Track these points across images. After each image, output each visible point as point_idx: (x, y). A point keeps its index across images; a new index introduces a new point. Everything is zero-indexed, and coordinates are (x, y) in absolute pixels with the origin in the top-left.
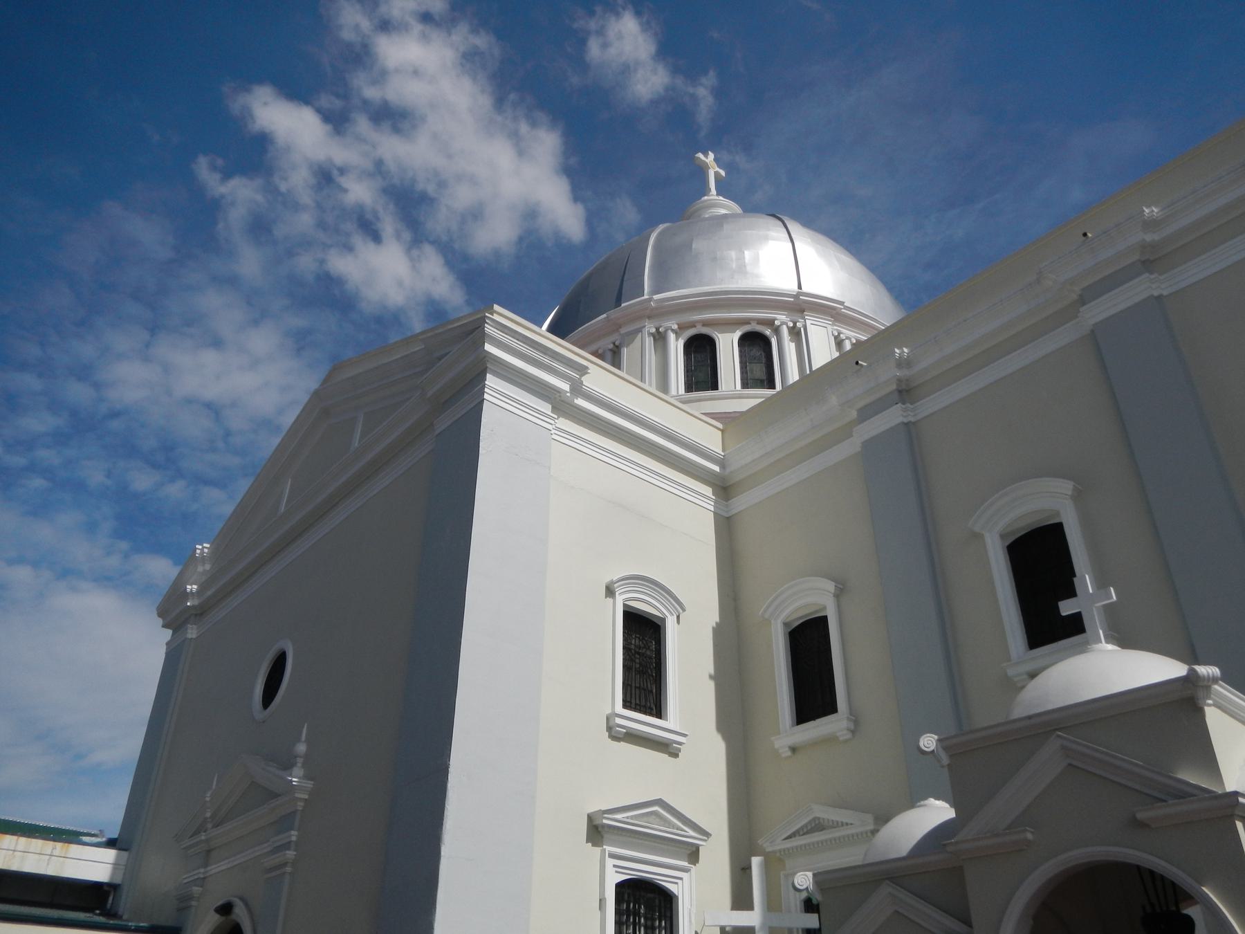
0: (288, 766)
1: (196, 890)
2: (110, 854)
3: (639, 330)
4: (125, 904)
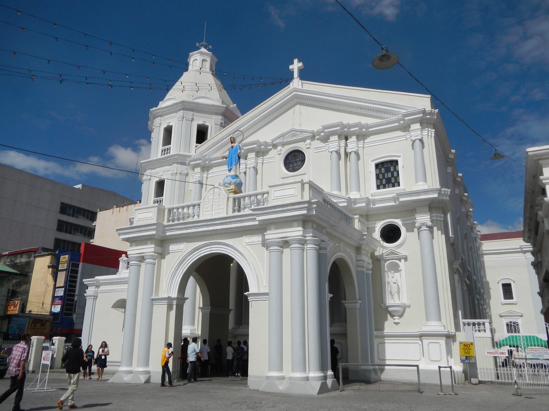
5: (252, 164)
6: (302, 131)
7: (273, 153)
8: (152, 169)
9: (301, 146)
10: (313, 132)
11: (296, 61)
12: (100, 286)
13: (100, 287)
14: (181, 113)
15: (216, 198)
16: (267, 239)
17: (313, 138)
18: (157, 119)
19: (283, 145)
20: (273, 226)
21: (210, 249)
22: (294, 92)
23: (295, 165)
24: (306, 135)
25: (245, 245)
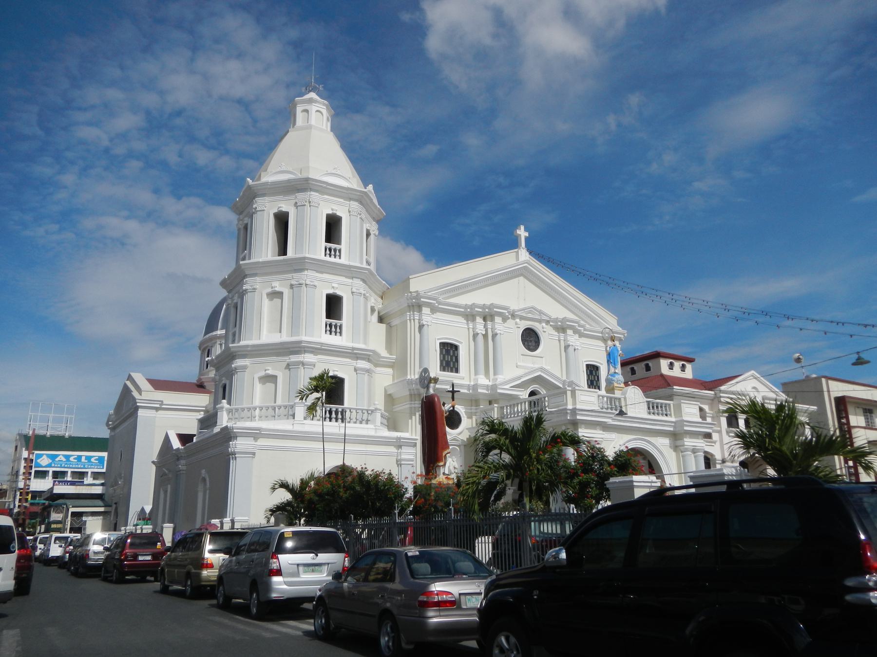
0: (121, 478)
1: (113, 498)
2: (101, 487)
3: (216, 343)
4: (106, 498)
5: (500, 330)
6: (541, 312)
7: (510, 322)
8: (317, 272)
9: (538, 327)
10: (550, 318)
11: (522, 227)
12: (259, 438)
13: (259, 440)
14: (355, 205)
15: (637, 398)
16: (684, 445)
17: (548, 322)
18: (312, 193)
19: (522, 318)
20: (688, 436)
21: (635, 444)
22: (524, 263)
23: (530, 344)
24: (544, 317)
25: (660, 444)
